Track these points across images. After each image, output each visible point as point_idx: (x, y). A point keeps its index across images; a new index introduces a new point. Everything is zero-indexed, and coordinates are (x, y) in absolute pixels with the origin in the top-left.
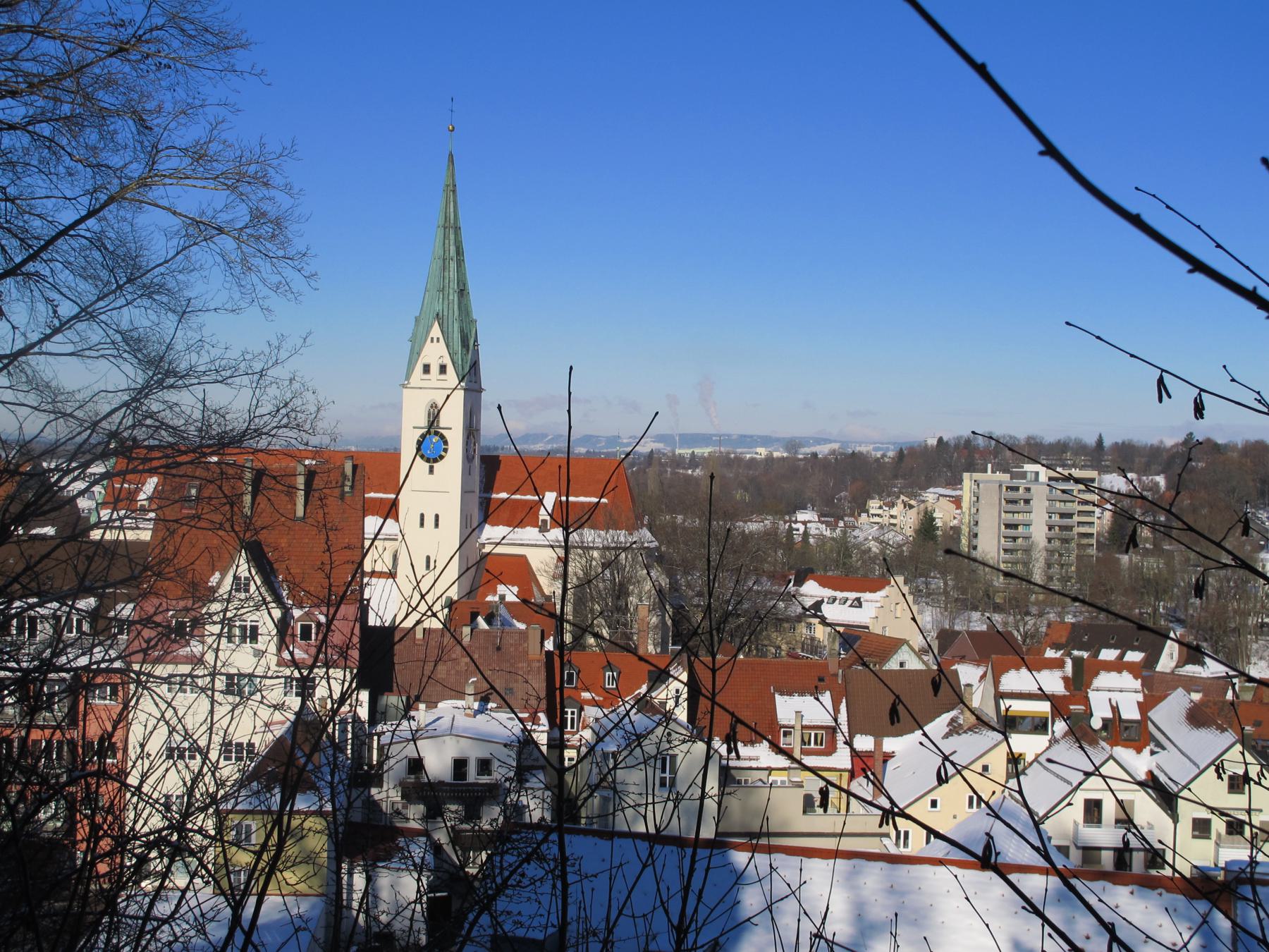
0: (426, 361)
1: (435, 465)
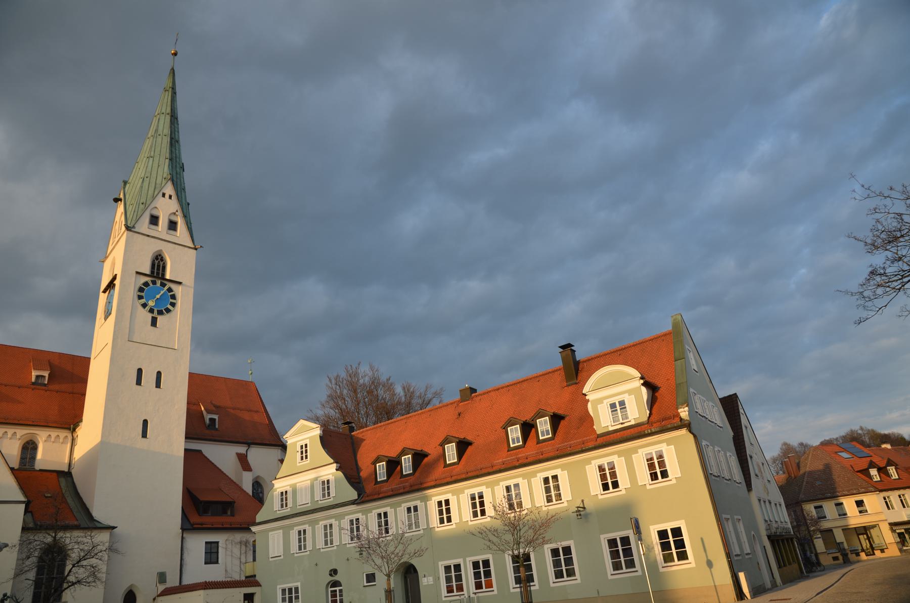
0: (155, 213)
1: (160, 319)
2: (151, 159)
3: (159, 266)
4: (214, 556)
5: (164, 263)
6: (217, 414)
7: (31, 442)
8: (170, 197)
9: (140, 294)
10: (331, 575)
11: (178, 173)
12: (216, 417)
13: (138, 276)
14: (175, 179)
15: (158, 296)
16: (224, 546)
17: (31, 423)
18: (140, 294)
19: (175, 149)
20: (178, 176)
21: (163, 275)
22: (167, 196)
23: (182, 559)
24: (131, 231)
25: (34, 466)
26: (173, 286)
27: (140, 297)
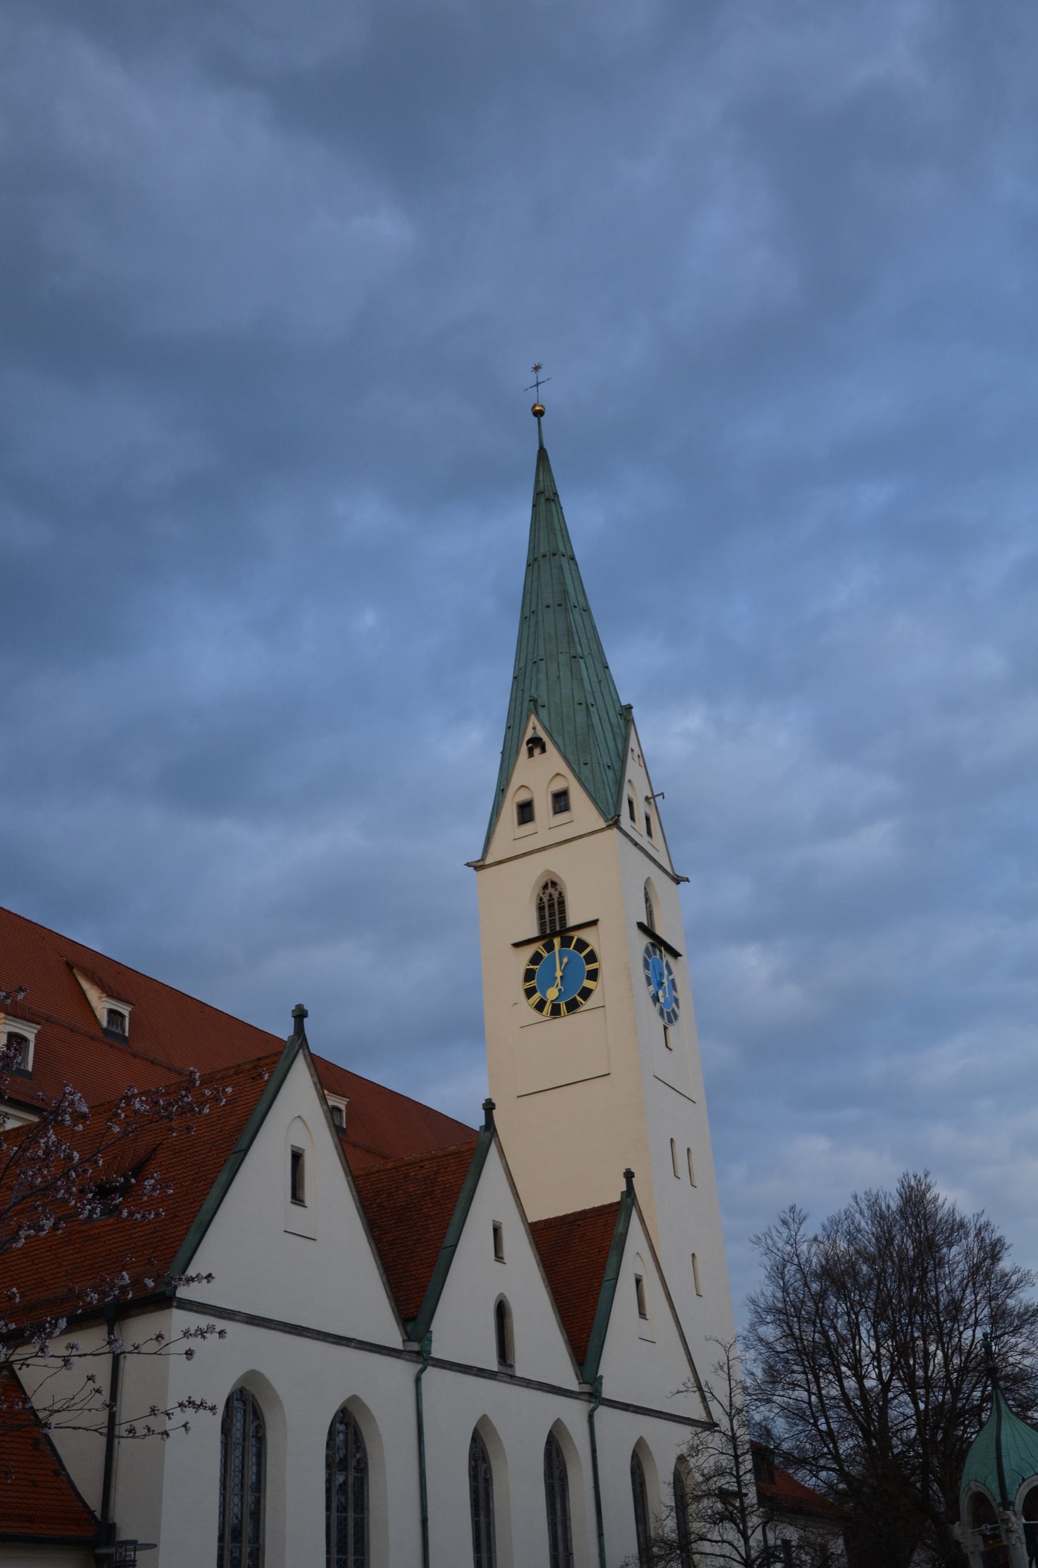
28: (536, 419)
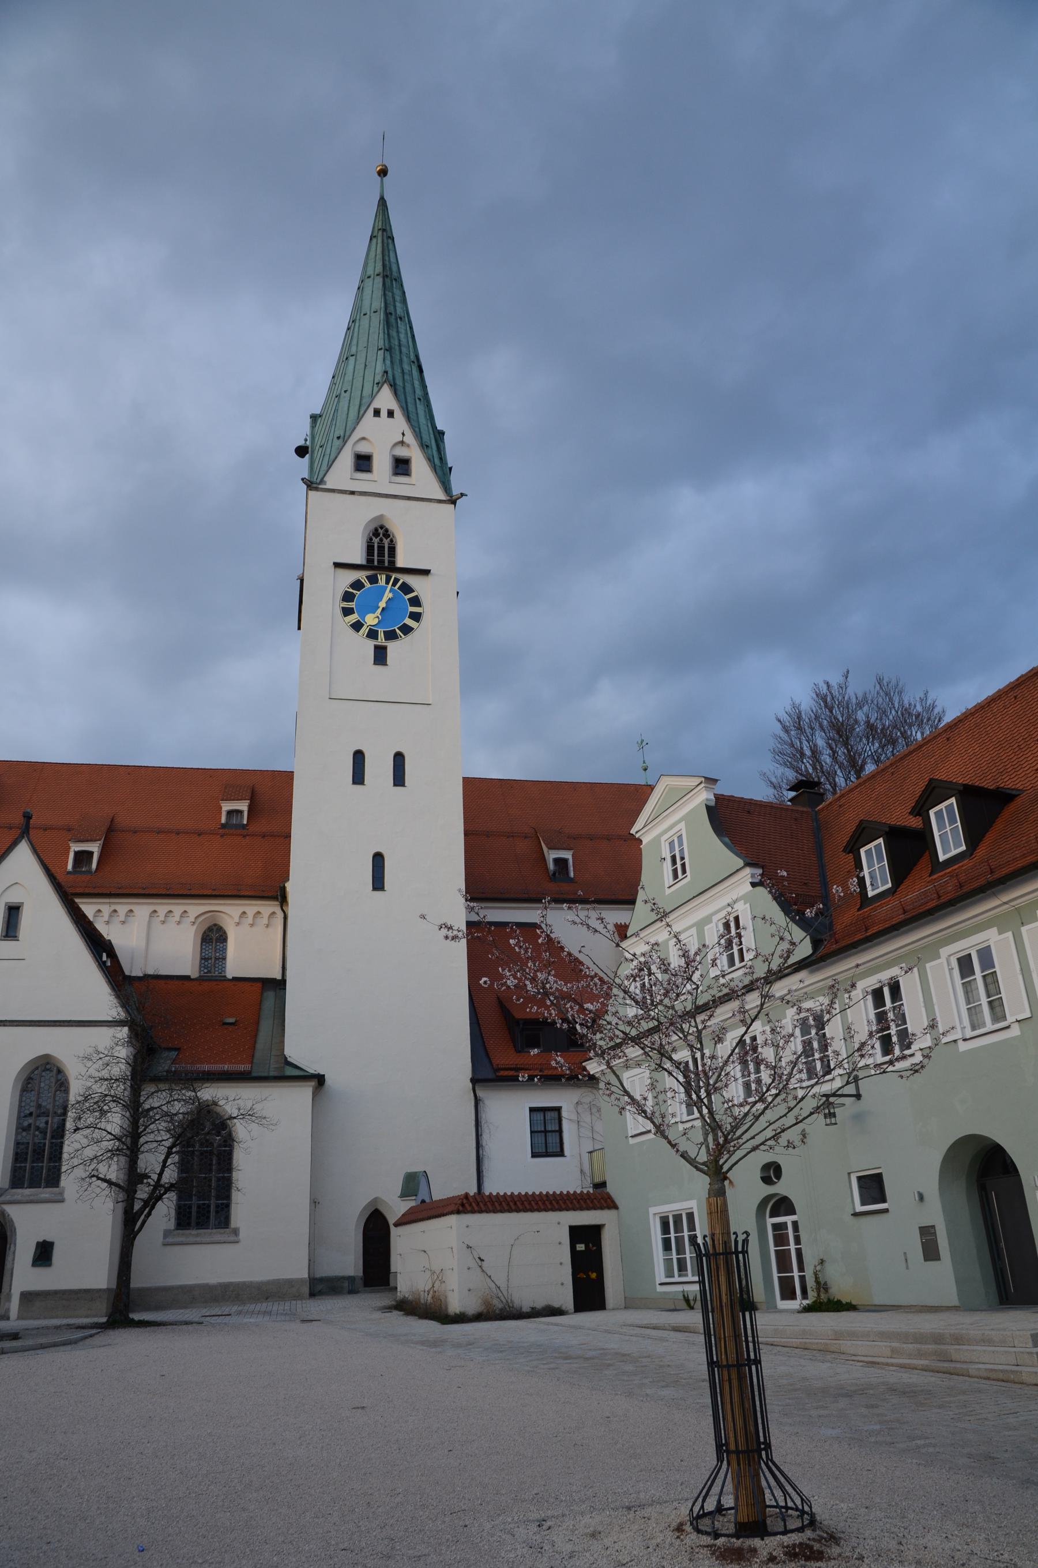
0: (363, 448)
1: (392, 647)
2: (352, 360)
3: (381, 548)
4: (552, 1139)
5: (392, 541)
6: (570, 849)
7: (215, 928)
8: (391, 414)
9: (345, 605)
10: (767, 1180)
11: (406, 371)
12: (567, 855)
13: (341, 572)
14: (399, 382)
15: (382, 604)
16: (574, 1117)
17: (209, 893)
18: (345, 605)
19: (398, 332)
20: (407, 377)
21: (392, 562)
22: (384, 413)
23: (478, 1146)
24: (317, 489)
25: (225, 971)
26: (411, 580)
27: (347, 612)
28: (380, 178)
